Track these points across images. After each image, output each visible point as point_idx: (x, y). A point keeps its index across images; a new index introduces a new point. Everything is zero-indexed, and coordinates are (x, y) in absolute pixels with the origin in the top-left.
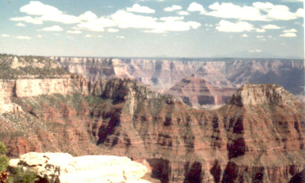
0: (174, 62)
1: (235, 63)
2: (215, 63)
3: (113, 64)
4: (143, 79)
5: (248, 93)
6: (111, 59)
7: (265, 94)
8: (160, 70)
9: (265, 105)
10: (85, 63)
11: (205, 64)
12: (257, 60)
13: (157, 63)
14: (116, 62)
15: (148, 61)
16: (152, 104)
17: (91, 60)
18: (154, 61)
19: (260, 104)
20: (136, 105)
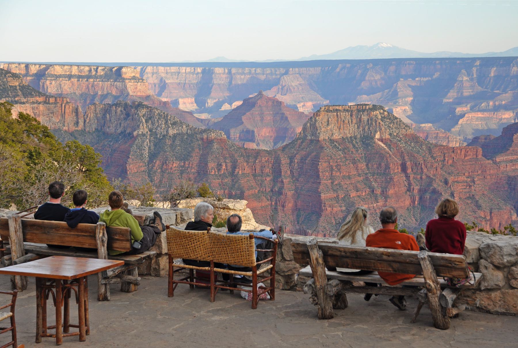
0: (234, 71)
1: (338, 70)
2: (303, 70)
3: (124, 76)
4: (181, 100)
5: (328, 121)
6: (120, 69)
7: (354, 121)
8: (211, 85)
9: (356, 139)
10: (75, 75)
11: (286, 73)
12: (376, 62)
13: (203, 72)
14: (127, 73)
15: (188, 69)
16: (178, 142)
17: (87, 68)
18: (199, 70)
19: (347, 137)
20: (152, 144)
